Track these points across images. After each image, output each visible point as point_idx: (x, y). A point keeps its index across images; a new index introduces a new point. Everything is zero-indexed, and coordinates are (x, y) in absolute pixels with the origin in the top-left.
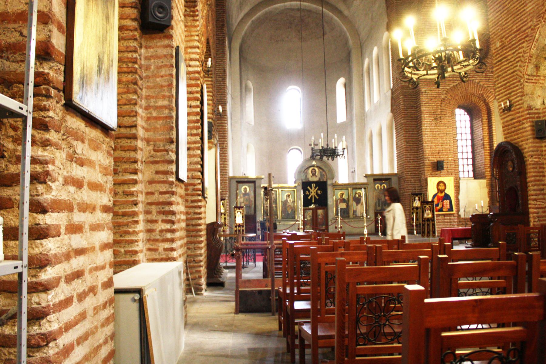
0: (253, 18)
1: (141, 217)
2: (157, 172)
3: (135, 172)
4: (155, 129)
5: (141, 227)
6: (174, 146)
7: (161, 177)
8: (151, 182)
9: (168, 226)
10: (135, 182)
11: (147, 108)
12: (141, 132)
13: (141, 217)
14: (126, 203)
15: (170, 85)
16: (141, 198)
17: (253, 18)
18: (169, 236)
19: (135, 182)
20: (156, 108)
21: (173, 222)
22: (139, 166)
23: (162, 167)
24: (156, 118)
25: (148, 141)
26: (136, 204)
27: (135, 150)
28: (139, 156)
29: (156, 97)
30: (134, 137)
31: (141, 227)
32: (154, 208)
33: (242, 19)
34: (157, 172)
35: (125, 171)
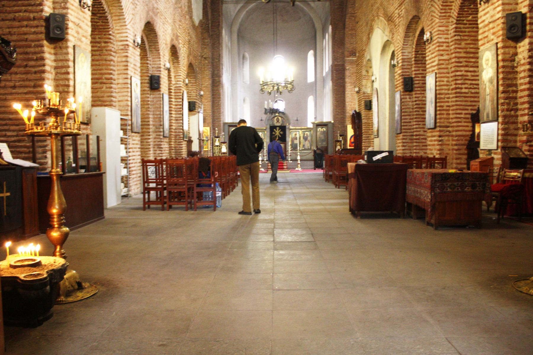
0: (247, 9)
1: (152, 149)
2: (157, 135)
3: (149, 136)
4: (156, 121)
5: (151, 152)
6: (162, 127)
7: (158, 137)
8: (155, 138)
9: (160, 152)
10: (149, 139)
11: (153, 115)
12: (151, 123)
13: (152, 149)
14: (146, 145)
15: (160, 107)
16: (151, 143)
17: (247, 9)
18: (161, 155)
19: (149, 139)
20: (157, 115)
21: (162, 151)
22: (151, 133)
23: (158, 134)
24: (156, 118)
25: (154, 125)
26: (150, 145)
27: (149, 129)
28: (151, 130)
29: (156, 111)
30: (149, 125)
31: (151, 152)
32: (156, 146)
33: (239, 10)
34: (157, 135)
35: (147, 135)
